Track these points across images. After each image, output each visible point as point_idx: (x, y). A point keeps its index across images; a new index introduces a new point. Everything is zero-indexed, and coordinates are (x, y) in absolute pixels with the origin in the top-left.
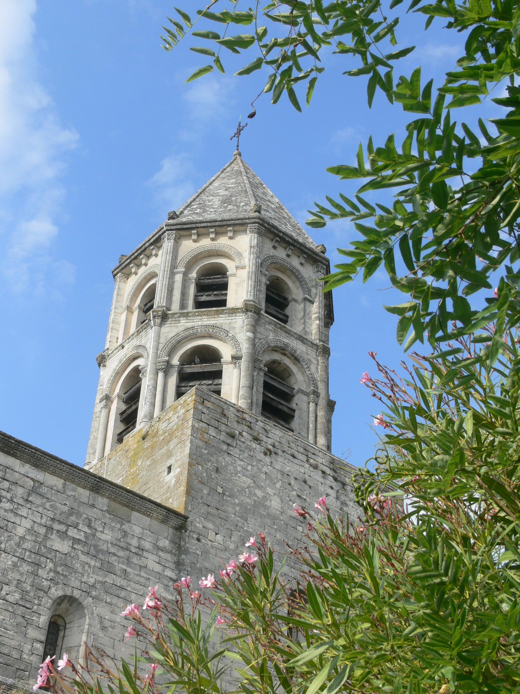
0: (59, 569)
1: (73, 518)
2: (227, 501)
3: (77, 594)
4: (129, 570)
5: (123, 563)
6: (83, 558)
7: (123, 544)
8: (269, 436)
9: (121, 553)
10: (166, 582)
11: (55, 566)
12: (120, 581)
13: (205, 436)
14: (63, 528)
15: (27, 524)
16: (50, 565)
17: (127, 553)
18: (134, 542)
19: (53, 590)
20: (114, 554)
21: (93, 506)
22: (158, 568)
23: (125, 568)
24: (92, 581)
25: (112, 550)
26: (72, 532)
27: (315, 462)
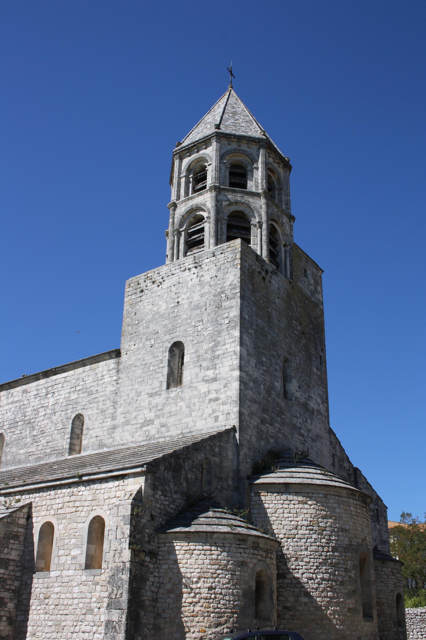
0: (74, 406)
1: (78, 382)
2: (140, 325)
3: (80, 412)
4: (98, 388)
5: (96, 387)
6: (82, 396)
7: (96, 379)
8: (160, 275)
9: (95, 383)
10: (112, 383)
11: (73, 406)
12: (94, 396)
13: (131, 301)
14: (74, 389)
15: (63, 396)
16: (71, 406)
17: (97, 382)
18: (100, 375)
19: (72, 416)
20: (93, 386)
21: (85, 371)
22: (110, 379)
23: (96, 389)
24: (85, 402)
25: (92, 384)
26: (78, 388)
27: (184, 268)
